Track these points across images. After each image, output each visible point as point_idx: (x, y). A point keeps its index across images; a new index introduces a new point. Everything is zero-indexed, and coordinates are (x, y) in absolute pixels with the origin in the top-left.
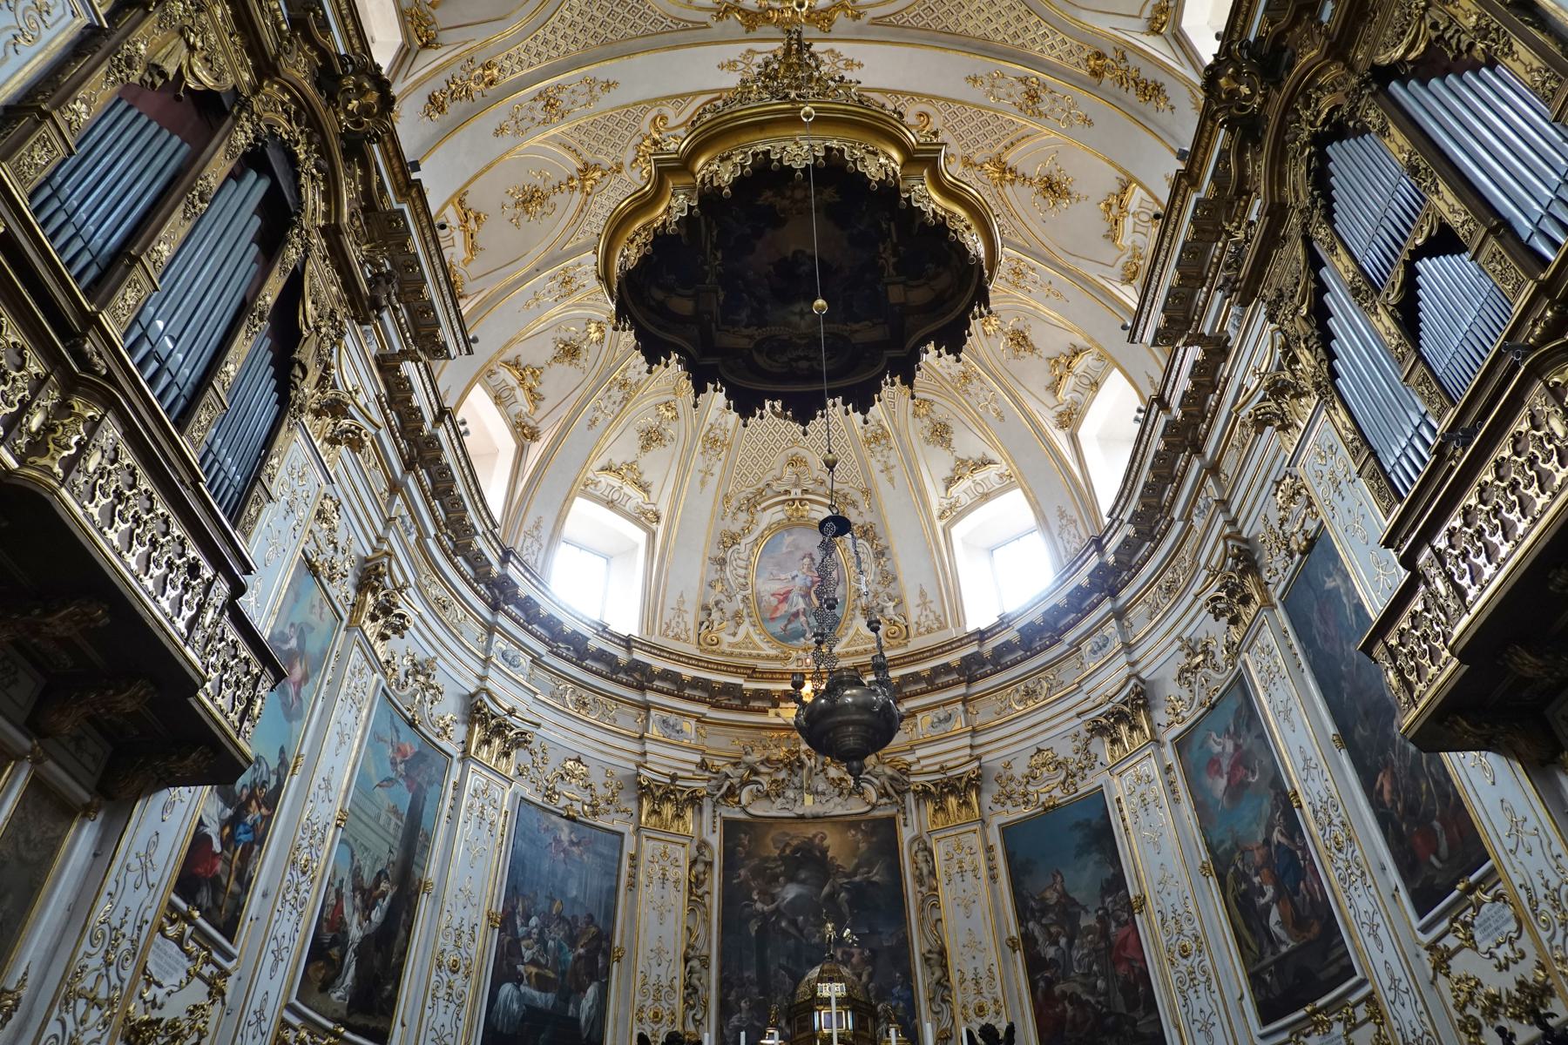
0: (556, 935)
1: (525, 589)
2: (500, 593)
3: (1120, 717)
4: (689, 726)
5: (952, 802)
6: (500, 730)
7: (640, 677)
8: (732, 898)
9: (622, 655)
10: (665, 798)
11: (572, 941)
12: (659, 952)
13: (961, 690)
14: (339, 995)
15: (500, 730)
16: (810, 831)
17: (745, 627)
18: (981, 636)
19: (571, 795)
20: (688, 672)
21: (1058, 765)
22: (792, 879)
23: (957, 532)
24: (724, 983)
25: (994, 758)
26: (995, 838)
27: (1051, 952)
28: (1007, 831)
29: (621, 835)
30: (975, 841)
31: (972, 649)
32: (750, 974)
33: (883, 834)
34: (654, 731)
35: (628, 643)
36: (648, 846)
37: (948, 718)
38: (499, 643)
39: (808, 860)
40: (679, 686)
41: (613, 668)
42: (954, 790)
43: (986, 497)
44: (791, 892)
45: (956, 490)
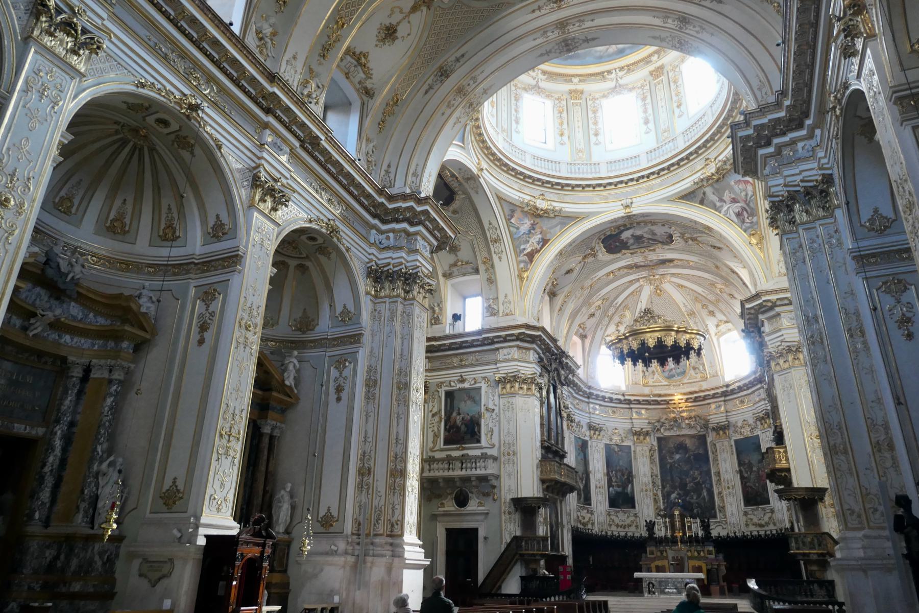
0: (619, 474)
1: (595, 392)
2: (589, 396)
3: (763, 418)
4: (643, 412)
5: (721, 432)
6: (596, 430)
7: (629, 402)
8: (662, 460)
9: (622, 398)
10: (640, 435)
11: (623, 475)
12: (645, 475)
13: (723, 399)
14: (582, 499)
15: (596, 430)
16: (682, 439)
17: (656, 376)
18: (727, 386)
19: (616, 439)
20: (641, 398)
21: (749, 425)
22: (677, 453)
23: (721, 339)
24: (662, 481)
25: (732, 420)
26: (733, 443)
27: (746, 475)
28: (736, 441)
29: (630, 447)
30: (726, 443)
31: (724, 389)
32: (669, 478)
33: (702, 439)
34: (634, 414)
35: (623, 395)
36: (639, 449)
37: (720, 406)
38: (591, 406)
39: (681, 447)
40: (639, 402)
41: (620, 402)
42: (721, 429)
43: (729, 330)
44: (677, 456)
45: (720, 328)
